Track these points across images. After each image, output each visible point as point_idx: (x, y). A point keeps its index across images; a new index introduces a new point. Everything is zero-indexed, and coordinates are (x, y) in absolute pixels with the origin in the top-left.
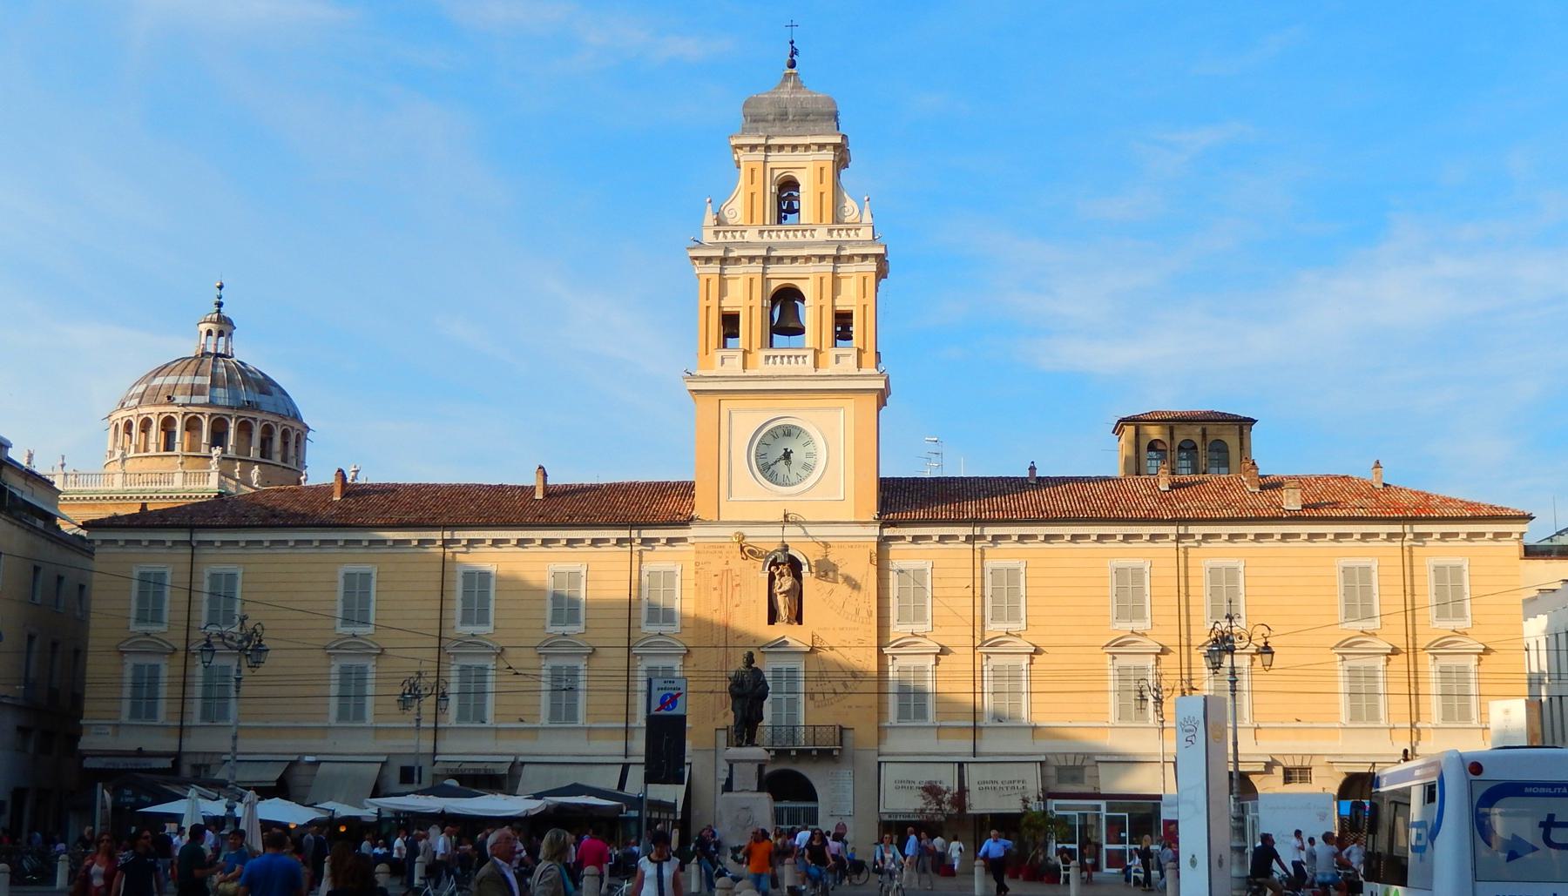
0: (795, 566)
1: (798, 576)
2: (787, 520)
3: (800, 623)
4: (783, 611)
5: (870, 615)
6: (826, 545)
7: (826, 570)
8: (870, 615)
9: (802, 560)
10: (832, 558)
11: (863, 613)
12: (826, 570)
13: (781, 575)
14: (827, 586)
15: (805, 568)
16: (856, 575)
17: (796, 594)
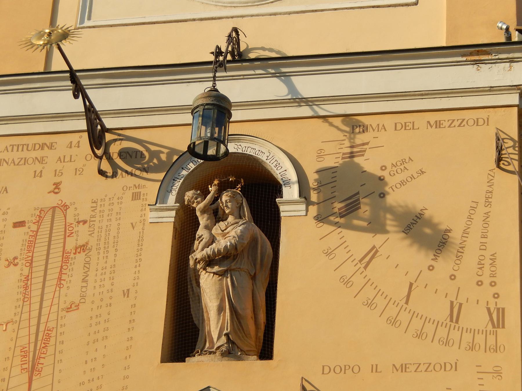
0: (260, 192)
1: (268, 219)
2: (233, 57)
3: (266, 352)
4: (215, 323)
5: (498, 319)
6: (353, 123)
7: (349, 196)
8: (498, 319)
9: (282, 169)
10: (369, 163)
11: (475, 318)
12: (349, 196)
13: (217, 215)
14: (359, 242)
15: (291, 192)
16: (444, 211)
17: (257, 267)
